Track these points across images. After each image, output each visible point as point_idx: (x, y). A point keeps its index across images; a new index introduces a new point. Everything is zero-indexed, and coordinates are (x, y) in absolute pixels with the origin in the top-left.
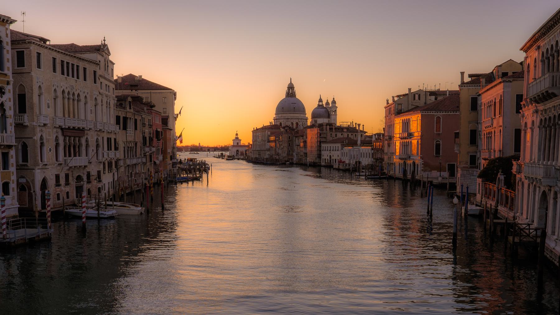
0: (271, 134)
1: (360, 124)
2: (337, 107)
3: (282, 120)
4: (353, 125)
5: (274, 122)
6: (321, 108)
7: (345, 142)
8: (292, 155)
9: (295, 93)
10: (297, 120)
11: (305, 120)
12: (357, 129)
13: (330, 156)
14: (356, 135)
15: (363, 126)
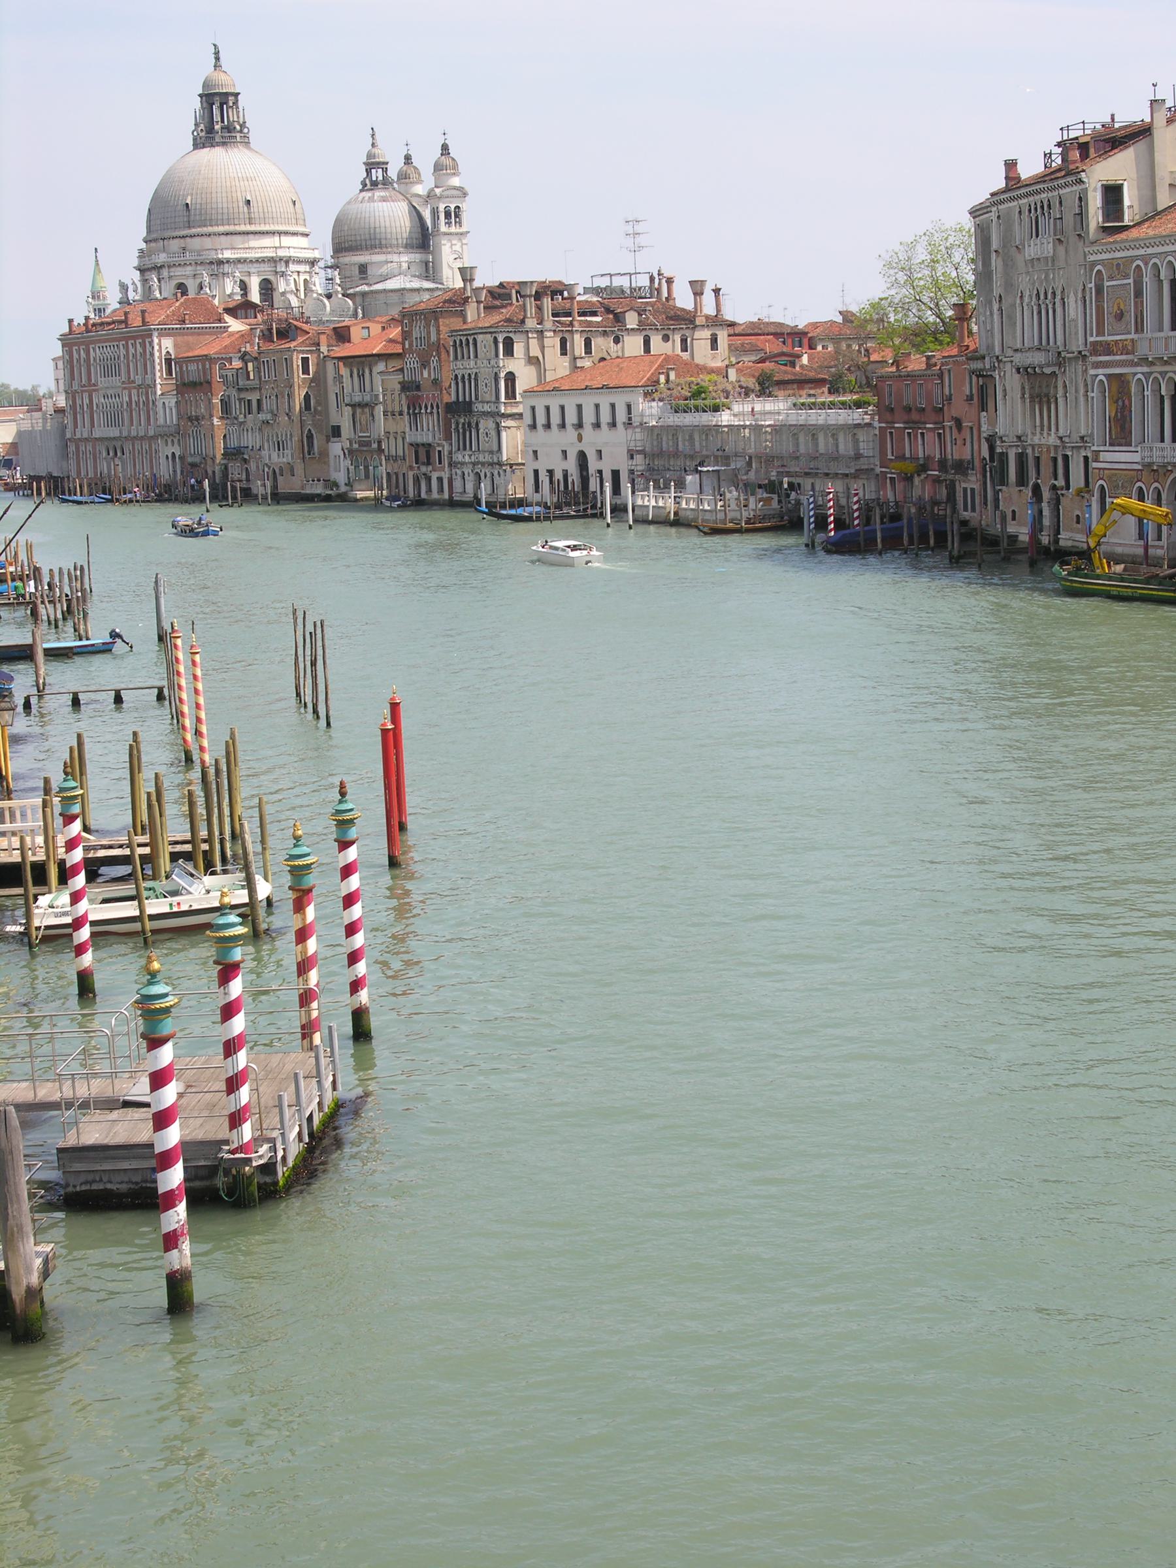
0: (176, 346)
1: (703, 282)
2: (464, 193)
3: (189, 270)
4: (659, 290)
5: (145, 281)
6: (384, 199)
7: (662, 379)
8: (324, 454)
9: (243, 125)
10: (266, 267)
11: (307, 268)
12: (684, 299)
13: (582, 457)
14: (684, 341)
15: (717, 291)
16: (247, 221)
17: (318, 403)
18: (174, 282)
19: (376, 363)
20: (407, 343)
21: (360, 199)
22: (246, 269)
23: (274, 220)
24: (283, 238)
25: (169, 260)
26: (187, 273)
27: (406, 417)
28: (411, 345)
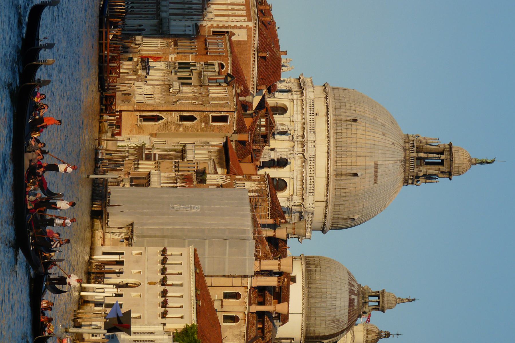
0: (239, 42)
3: (298, 117)
6: (351, 301)
16: (338, 172)
17: (186, 128)
18: (287, 103)
19: (222, 167)
20: (241, 177)
21: (352, 282)
22: (296, 168)
23: (337, 198)
24: (324, 204)
25: (308, 101)
26: (295, 116)
27: (173, 174)
28: (239, 180)
